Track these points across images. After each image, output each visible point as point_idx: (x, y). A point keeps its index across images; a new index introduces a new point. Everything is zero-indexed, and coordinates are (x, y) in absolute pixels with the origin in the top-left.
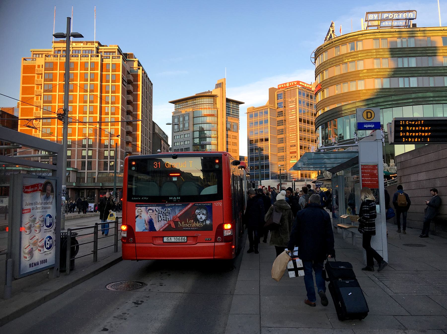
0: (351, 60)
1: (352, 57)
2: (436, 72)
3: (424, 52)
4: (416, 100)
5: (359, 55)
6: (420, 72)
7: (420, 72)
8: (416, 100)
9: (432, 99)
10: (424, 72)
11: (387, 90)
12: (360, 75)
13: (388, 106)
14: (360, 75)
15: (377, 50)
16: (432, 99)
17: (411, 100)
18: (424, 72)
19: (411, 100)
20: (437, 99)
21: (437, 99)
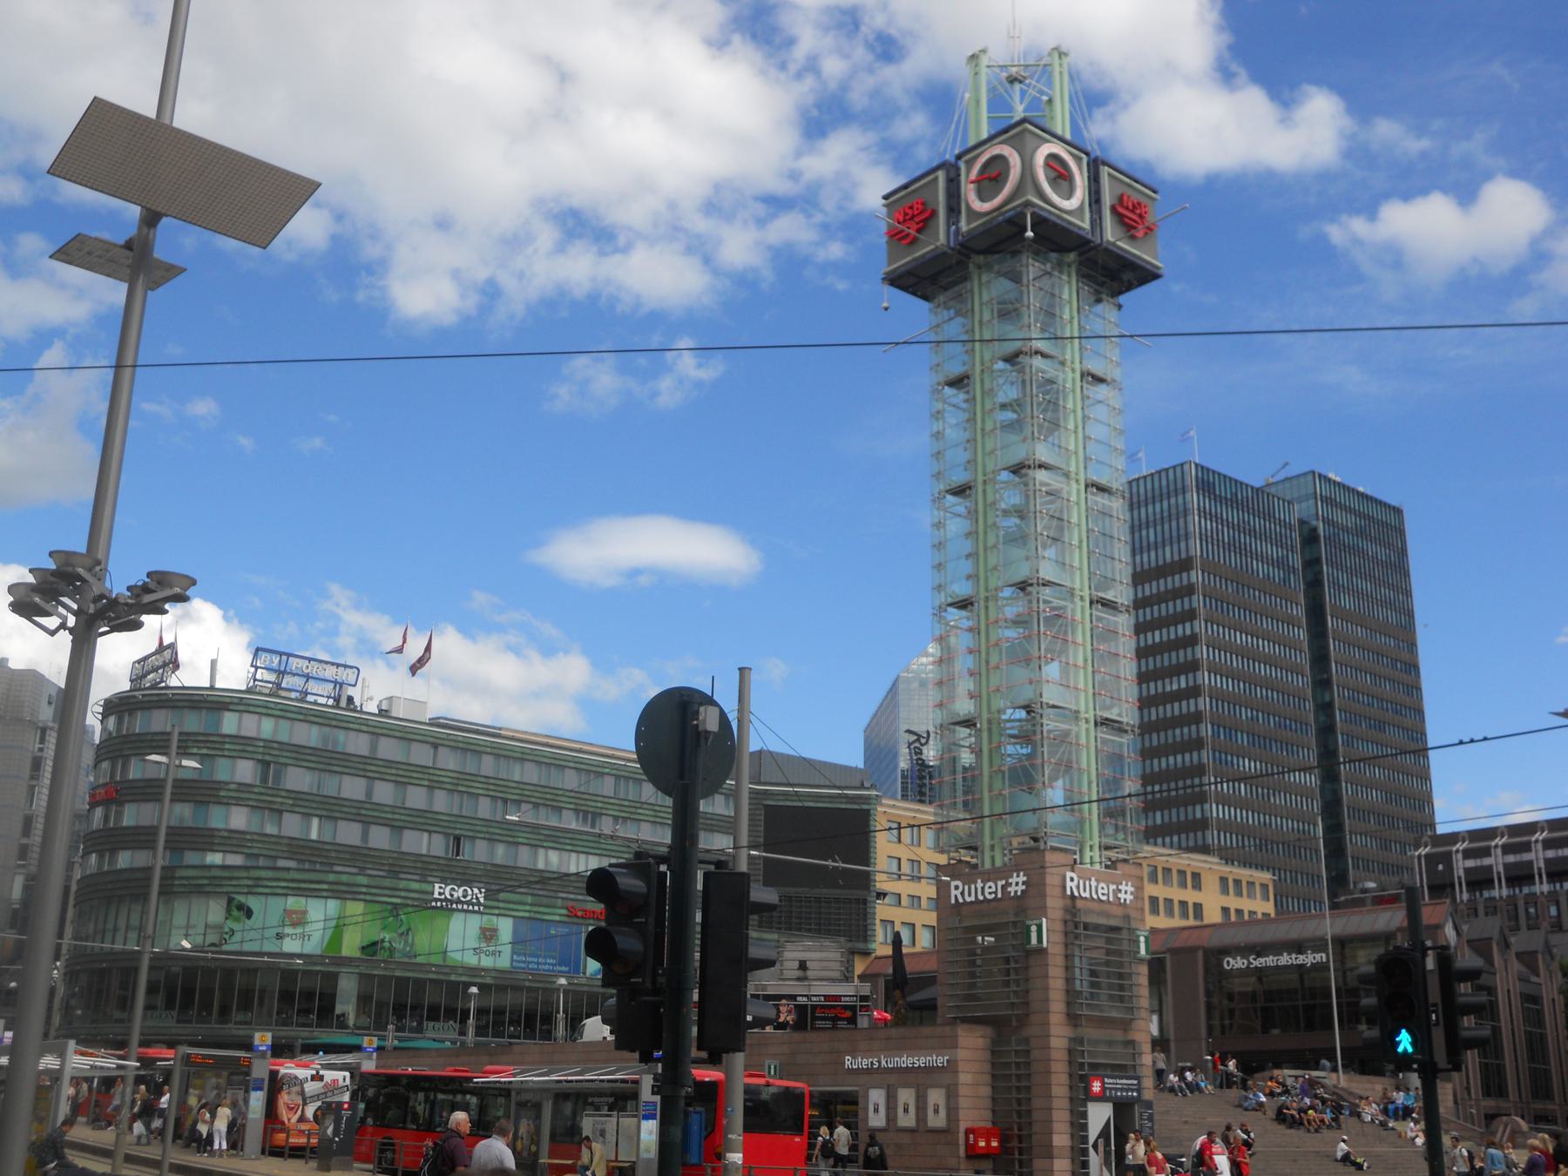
0: (205, 751)
1: (209, 745)
2: (376, 814)
3: (361, 766)
4: (335, 887)
5: (227, 746)
6: (345, 809)
7: (345, 809)
8: (335, 887)
9: (364, 890)
10: (353, 811)
11: (272, 840)
12: (222, 793)
13: (279, 891)
14: (222, 793)
15: (267, 744)
16: (364, 890)
17: (325, 887)
18: (353, 811)
19: (325, 887)
20: (373, 891)
21: (373, 891)
